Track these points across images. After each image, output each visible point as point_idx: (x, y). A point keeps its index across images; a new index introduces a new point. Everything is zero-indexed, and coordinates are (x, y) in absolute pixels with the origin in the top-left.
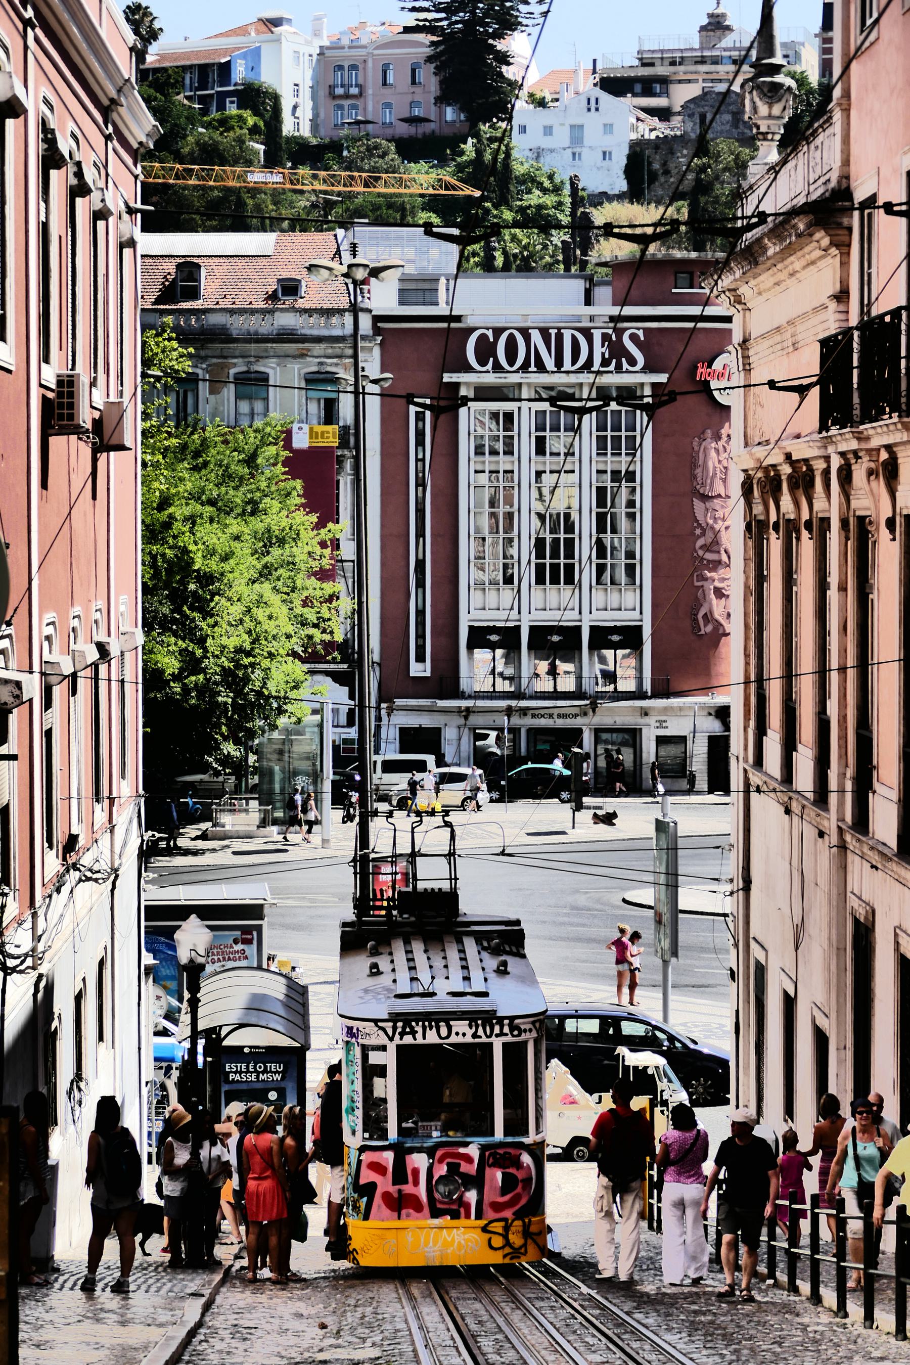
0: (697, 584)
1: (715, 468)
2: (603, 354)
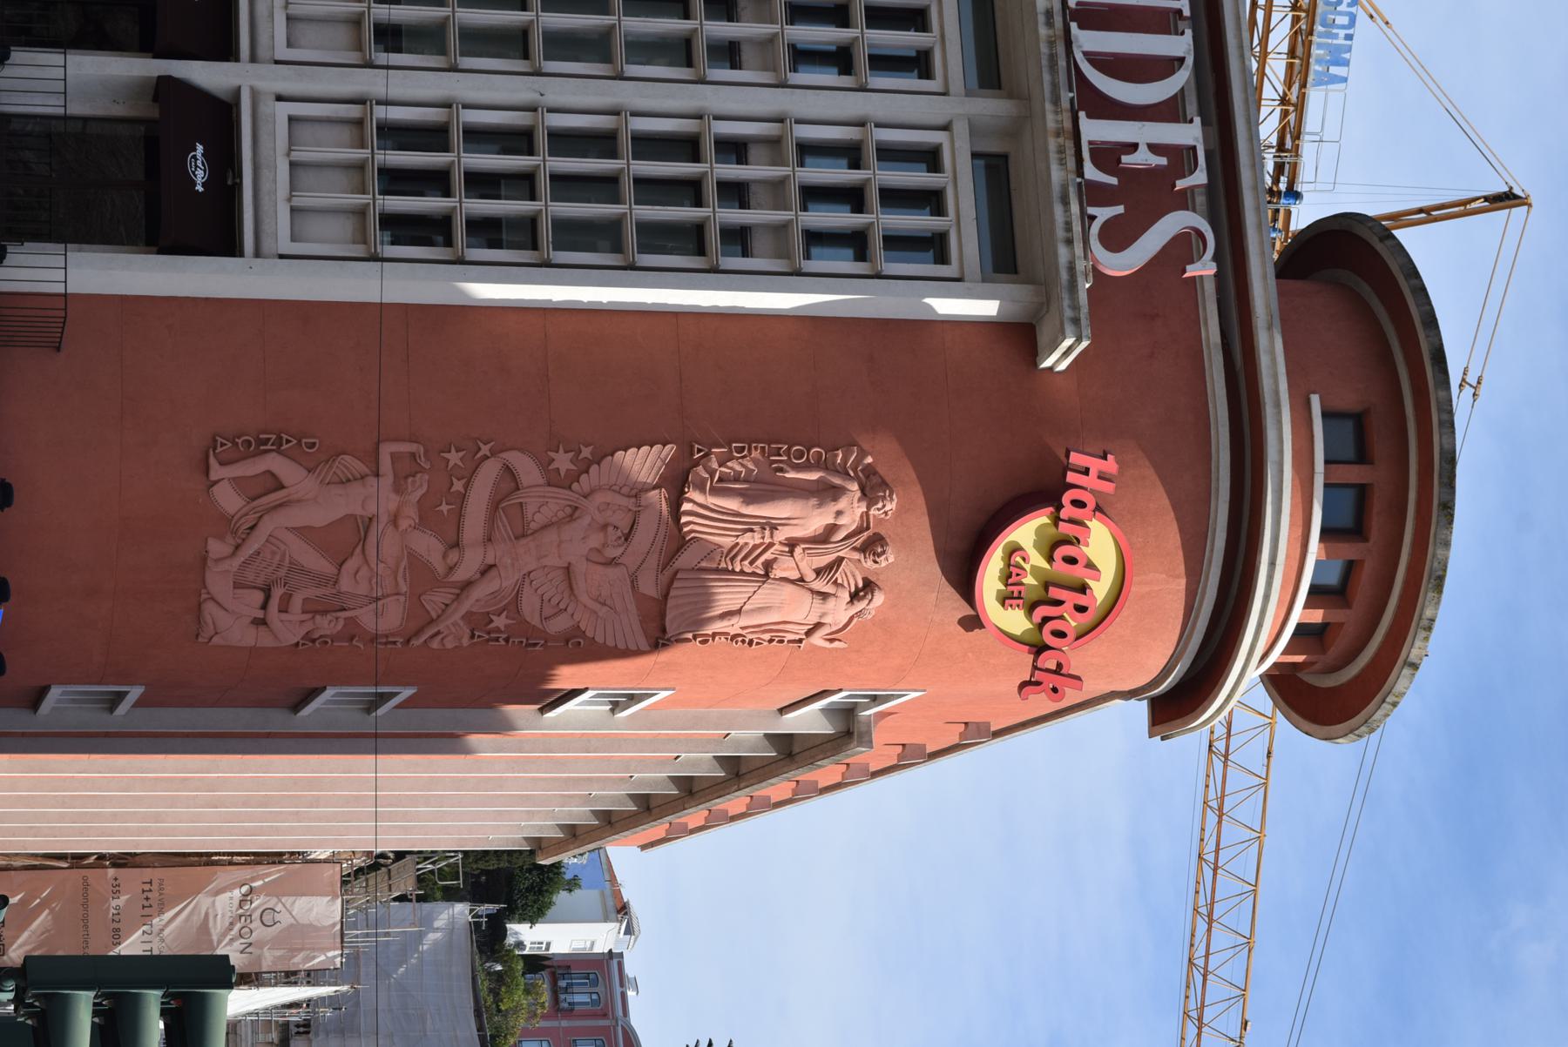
0: (386, 450)
2: (1134, 147)
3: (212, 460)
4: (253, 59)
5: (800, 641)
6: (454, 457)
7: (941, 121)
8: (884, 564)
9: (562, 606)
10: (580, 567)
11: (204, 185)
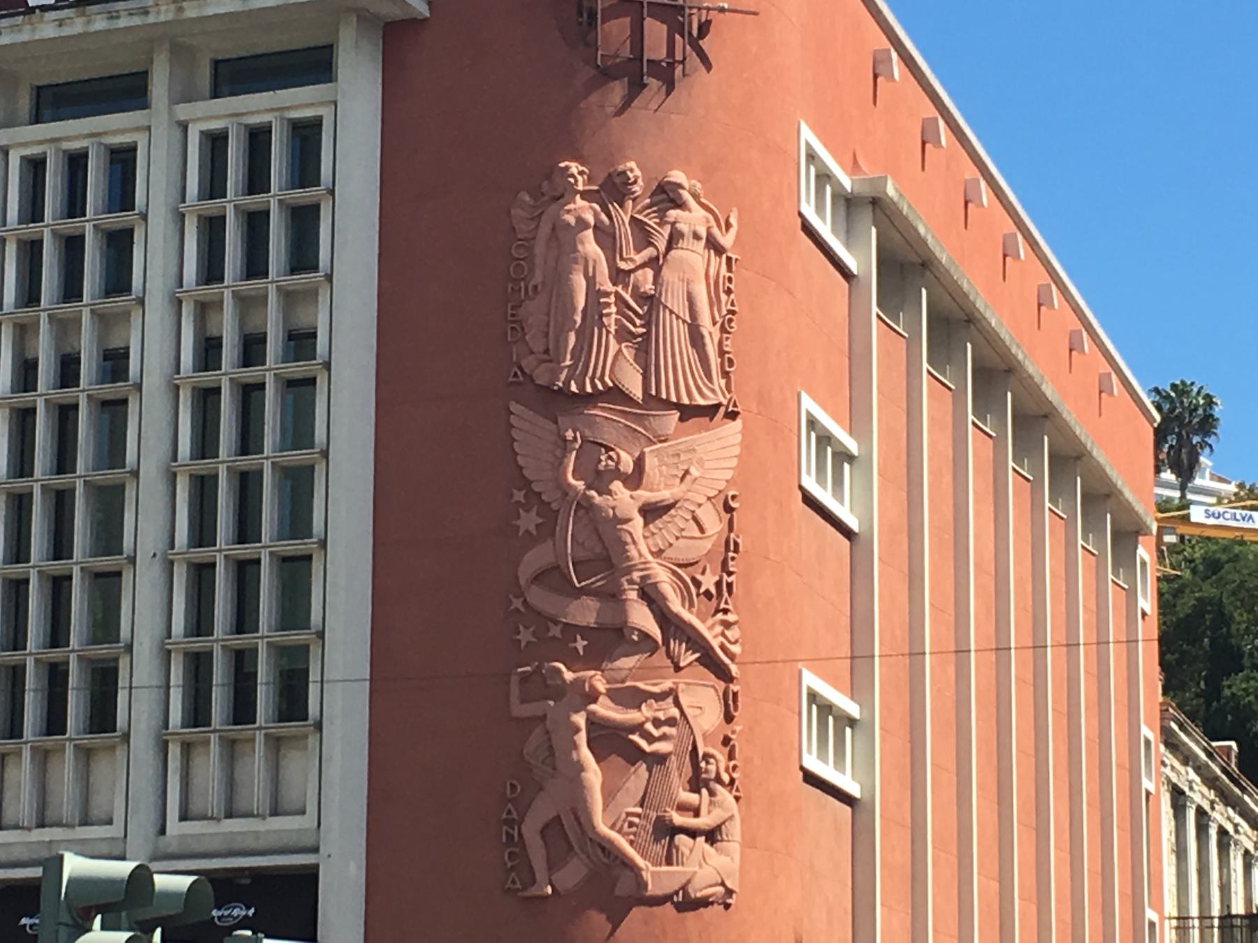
0: (520, 710)
1: (594, 294)
3: (527, 894)
4: (315, 850)
5: (729, 259)
6: (525, 636)
7: (178, 133)
8: (638, 172)
9: (689, 517)
10: (644, 495)
11: (248, 908)
